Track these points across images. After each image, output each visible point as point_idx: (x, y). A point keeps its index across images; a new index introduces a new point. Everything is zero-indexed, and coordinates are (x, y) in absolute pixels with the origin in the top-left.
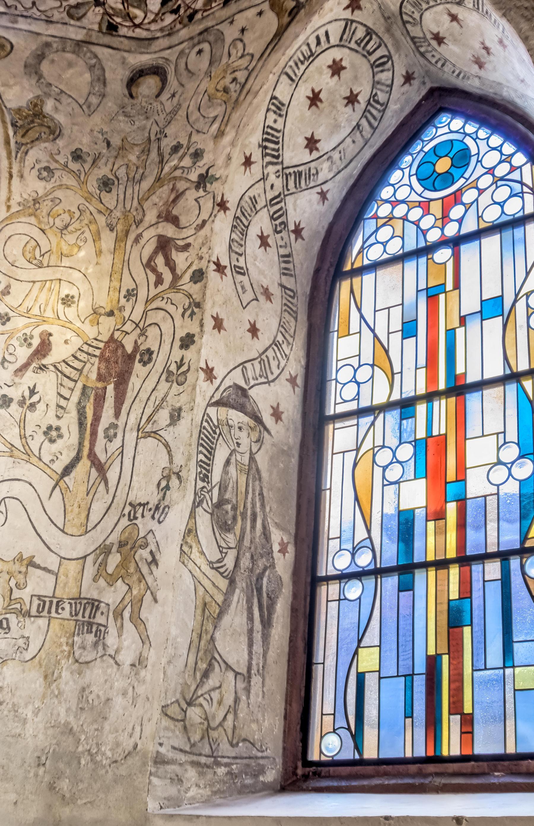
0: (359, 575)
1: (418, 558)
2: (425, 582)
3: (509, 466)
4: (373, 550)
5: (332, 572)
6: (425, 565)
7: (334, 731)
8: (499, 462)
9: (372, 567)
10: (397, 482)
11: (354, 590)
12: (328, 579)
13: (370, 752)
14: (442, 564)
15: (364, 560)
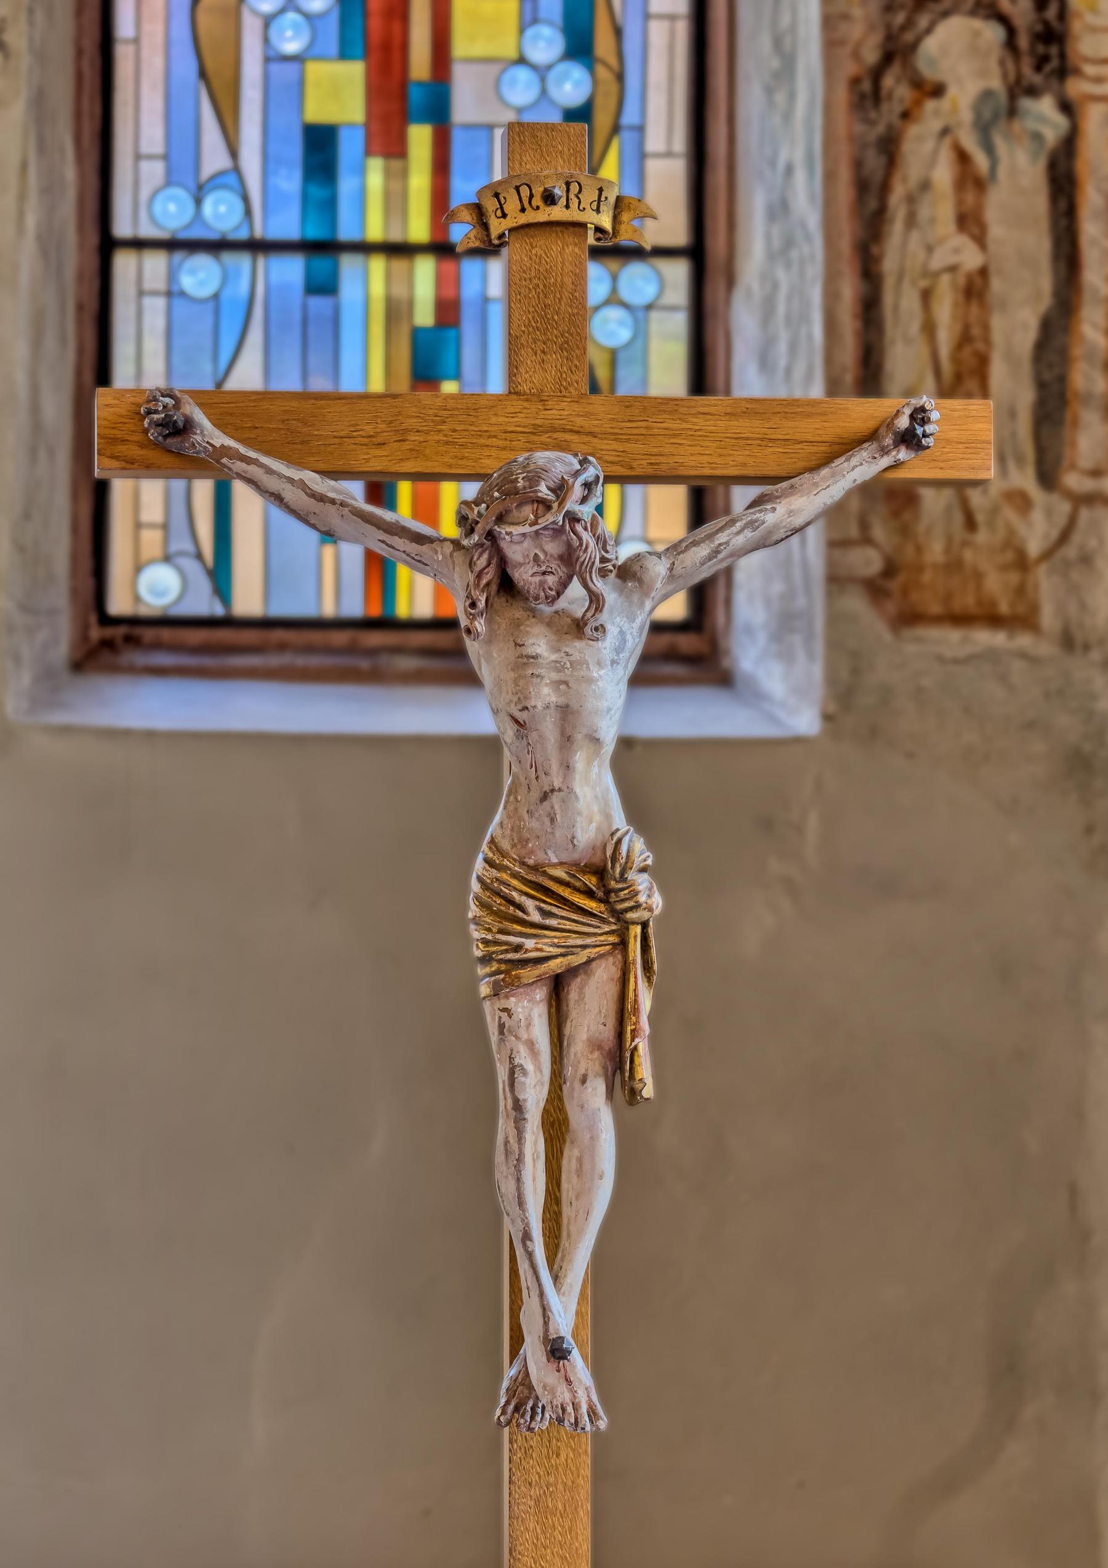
0: (217, 246)
1: (346, 232)
2: (367, 282)
3: (542, 72)
4: (246, 199)
5: (147, 231)
6: (365, 248)
7: (167, 559)
8: (521, 60)
9: (243, 235)
10: (298, 59)
11: (200, 275)
12: (139, 244)
13: (248, 600)
14: (398, 250)
15: (221, 214)
